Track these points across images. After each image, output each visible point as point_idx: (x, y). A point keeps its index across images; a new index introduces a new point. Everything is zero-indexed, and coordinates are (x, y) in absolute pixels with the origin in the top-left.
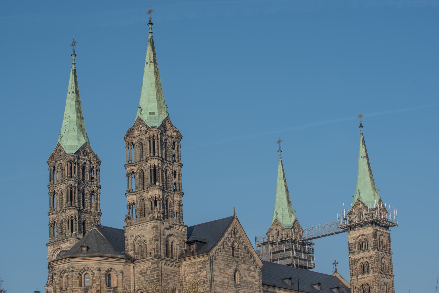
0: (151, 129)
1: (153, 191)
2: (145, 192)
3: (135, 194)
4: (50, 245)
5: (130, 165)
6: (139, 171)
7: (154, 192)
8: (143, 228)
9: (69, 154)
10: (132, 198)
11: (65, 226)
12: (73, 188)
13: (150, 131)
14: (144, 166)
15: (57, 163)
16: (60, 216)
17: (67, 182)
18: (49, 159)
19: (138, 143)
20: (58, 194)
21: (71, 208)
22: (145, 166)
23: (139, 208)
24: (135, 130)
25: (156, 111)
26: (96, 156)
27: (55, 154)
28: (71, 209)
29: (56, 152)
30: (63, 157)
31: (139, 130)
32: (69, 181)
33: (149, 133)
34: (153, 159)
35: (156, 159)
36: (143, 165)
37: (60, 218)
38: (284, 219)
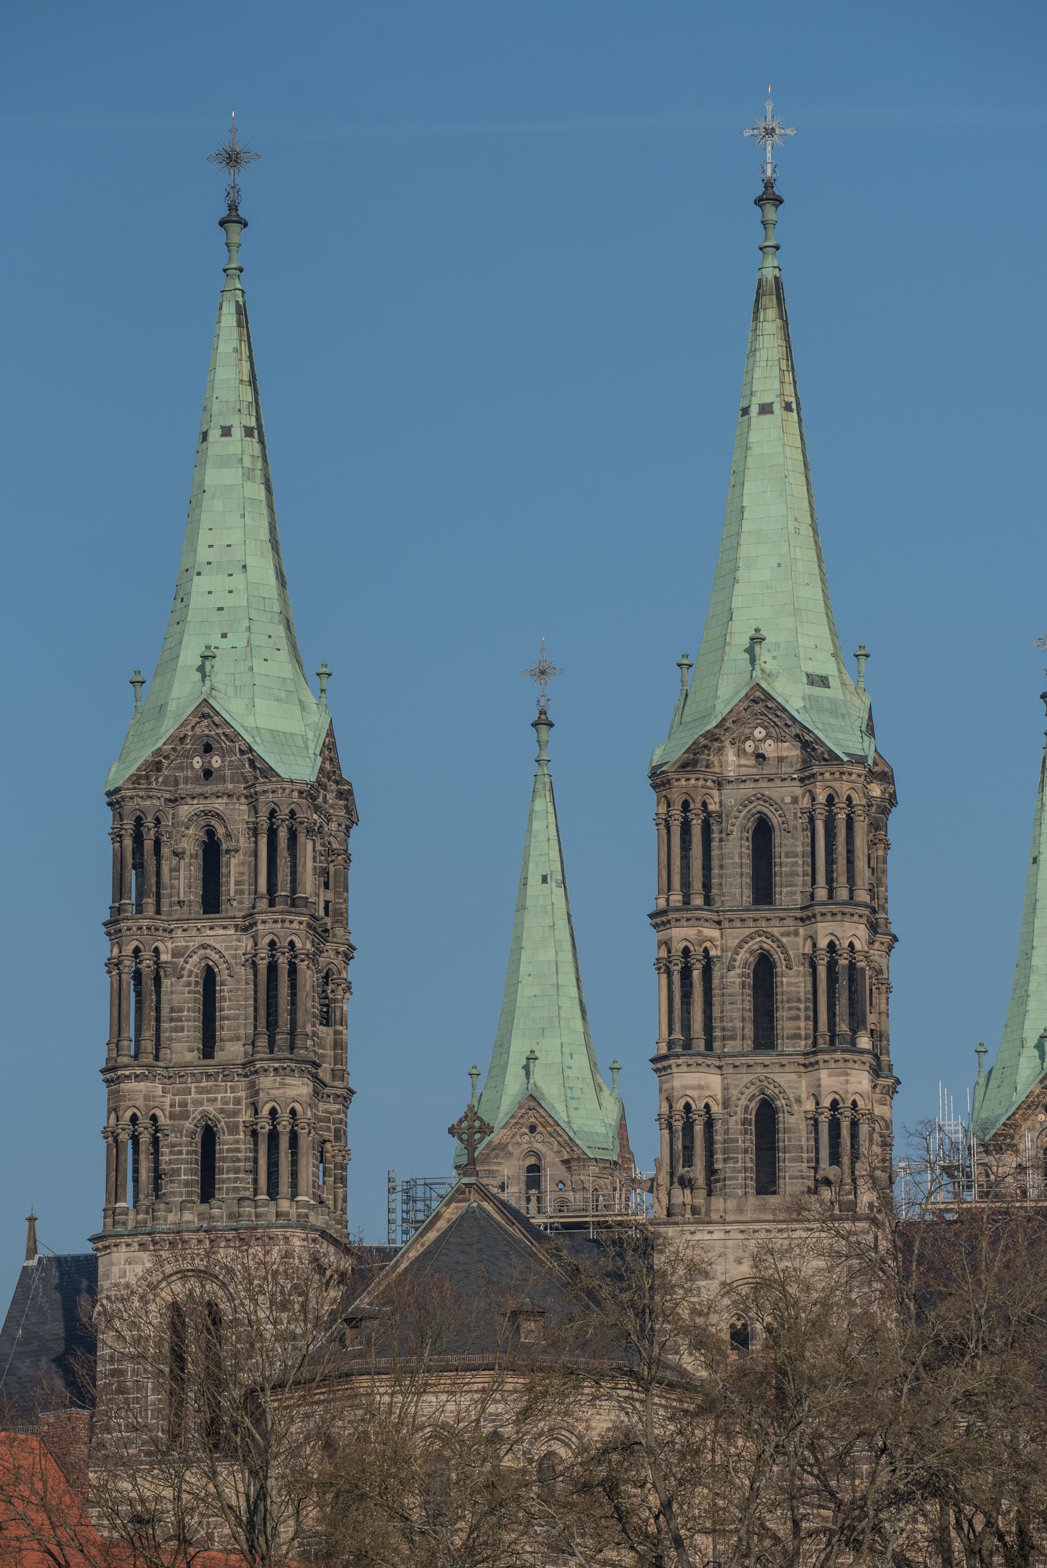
0: (847, 768)
1: (847, 1074)
2: (787, 1069)
3: (720, 1068)
4: (128, 1245)
5: (697, 919)
6: (743, 955)
7: (852, 1079)
9: (292, 782)
10: (702, 1083)
11: (228, 1150)
12: (302, 961)
13: (837, 775)
14: (783, 934)
15: (185, 811)
16: (216, 1099)
17: (268, 926)
18: (133, 775)
19: (743, 814)
20: (185, 972)
21: (293, 1065)
22: (784, 940)
23: (740, 1138)
24: (727, 743)
26: (350, 792)
27: (172, 757)
28: (293, 1071)
29: (179, 748)
30: (230, 786)
31: (750, 750)
32: (283, 921)
33: (829, 784)
34: (848, 916)
35: (861, 920)
36: (776, 931)
37: (198, 1103)
38: (572, 1104)
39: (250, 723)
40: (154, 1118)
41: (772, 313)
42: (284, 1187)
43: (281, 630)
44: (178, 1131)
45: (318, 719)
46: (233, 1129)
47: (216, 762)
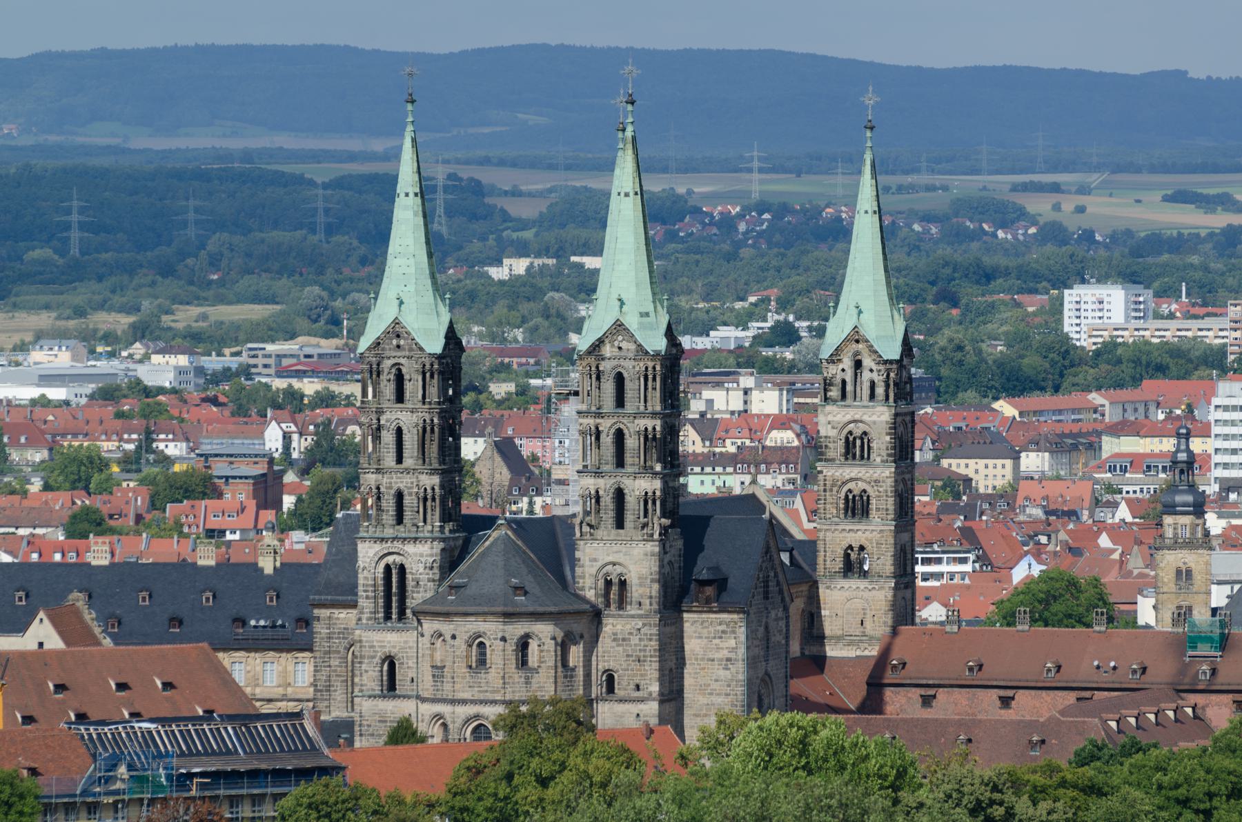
6: (613, 431)
8: (624, 550)
25: (650, 308)
36: (625, 421)
39: (416, 326)
40: (378, 488)
41: (630, 152)
42: (429, 520)
43: (429, 282)
44: (389, 494)
45: (446, 318)
46: (410, 494)
47: (402, 342)
